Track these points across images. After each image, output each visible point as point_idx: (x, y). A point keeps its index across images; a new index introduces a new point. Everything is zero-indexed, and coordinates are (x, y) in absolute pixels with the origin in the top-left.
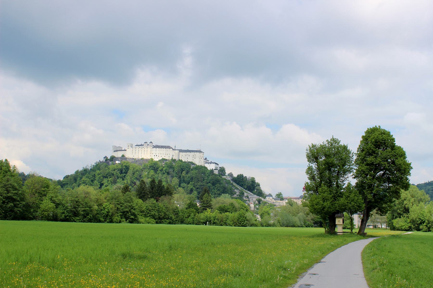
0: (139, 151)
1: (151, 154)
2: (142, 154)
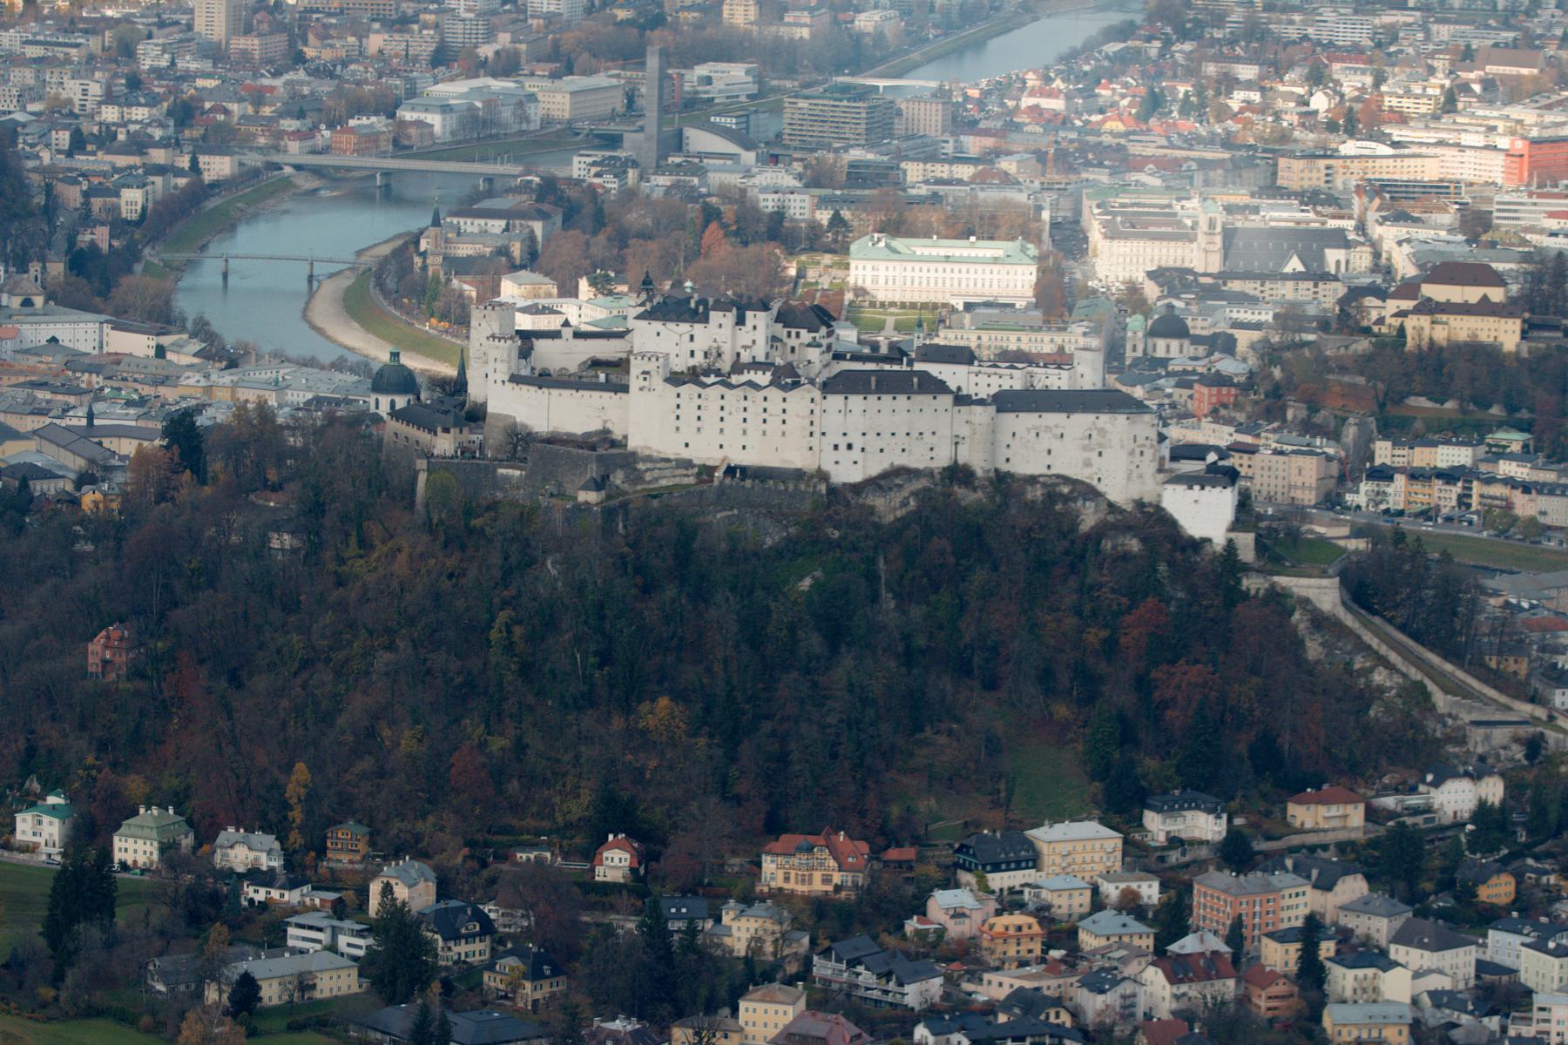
0: (722, 414)
1: (811, 434)
2: (745, 432)
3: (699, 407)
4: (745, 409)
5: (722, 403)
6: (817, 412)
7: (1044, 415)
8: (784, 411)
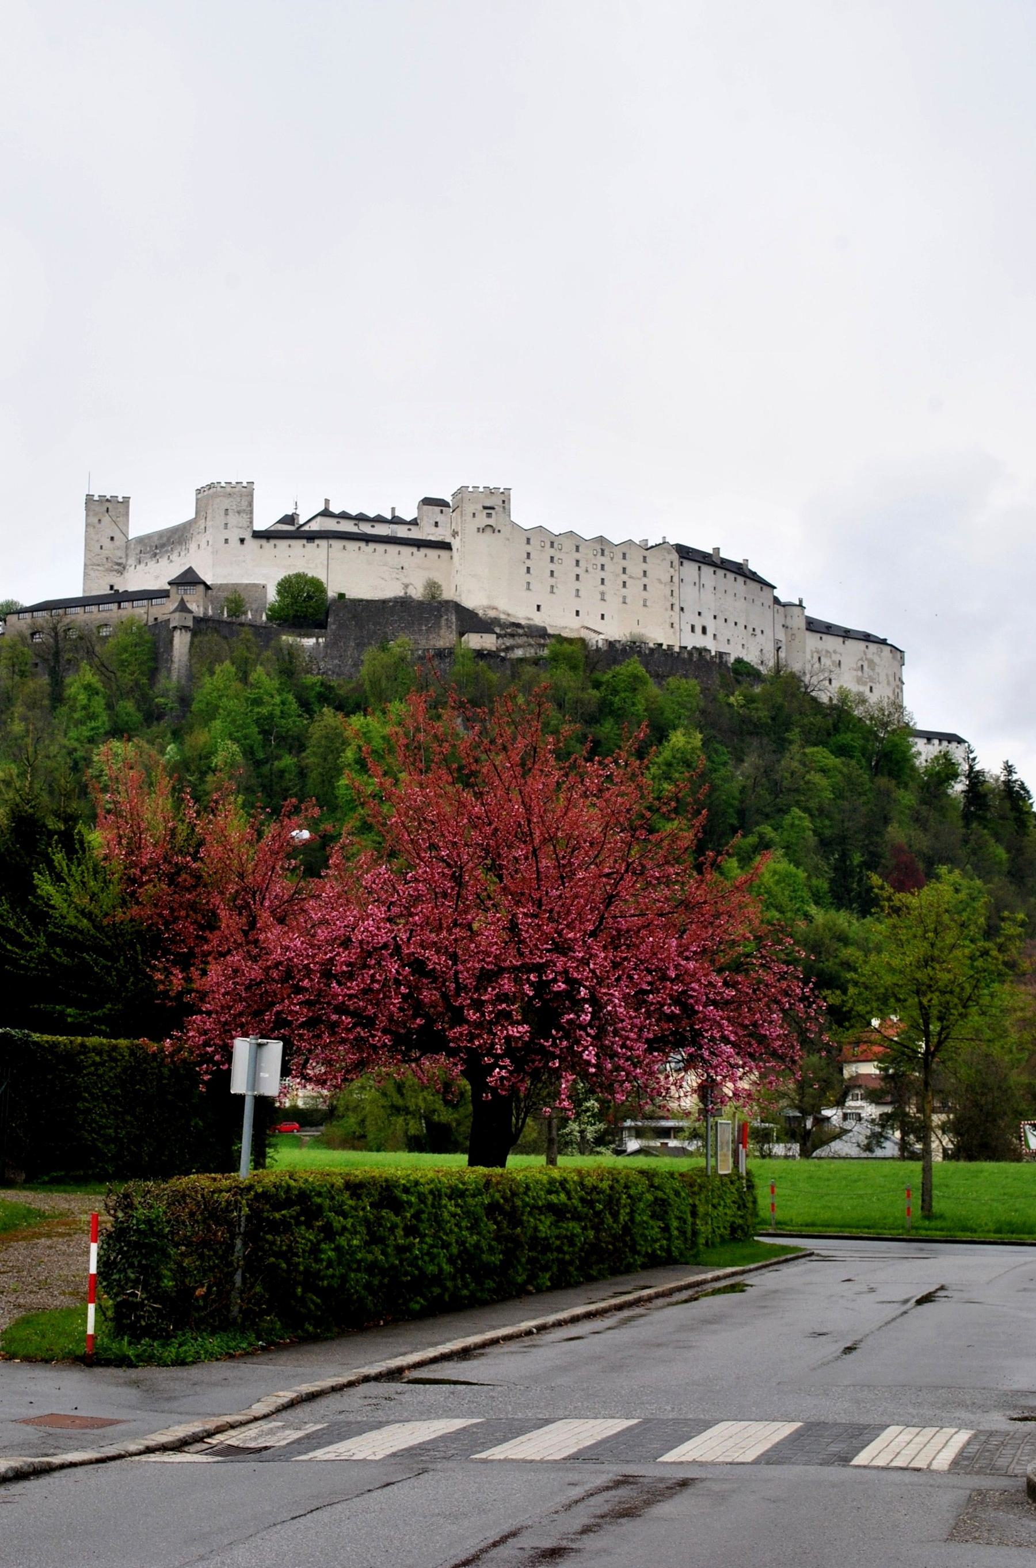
0: (578, 571)
3: (552, 558)
5: (577, 556)
6: (676, 579)
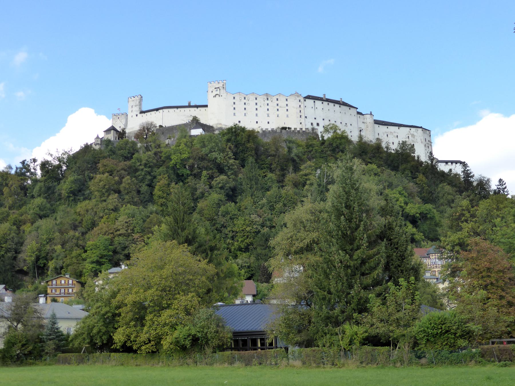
0: (256, 107)
2: (268, 116)
3: (245, 104)
4: (268, 104)
5: (256, 101)
6: (302, 106)
7: (389, 127)
8: (287, 105)
